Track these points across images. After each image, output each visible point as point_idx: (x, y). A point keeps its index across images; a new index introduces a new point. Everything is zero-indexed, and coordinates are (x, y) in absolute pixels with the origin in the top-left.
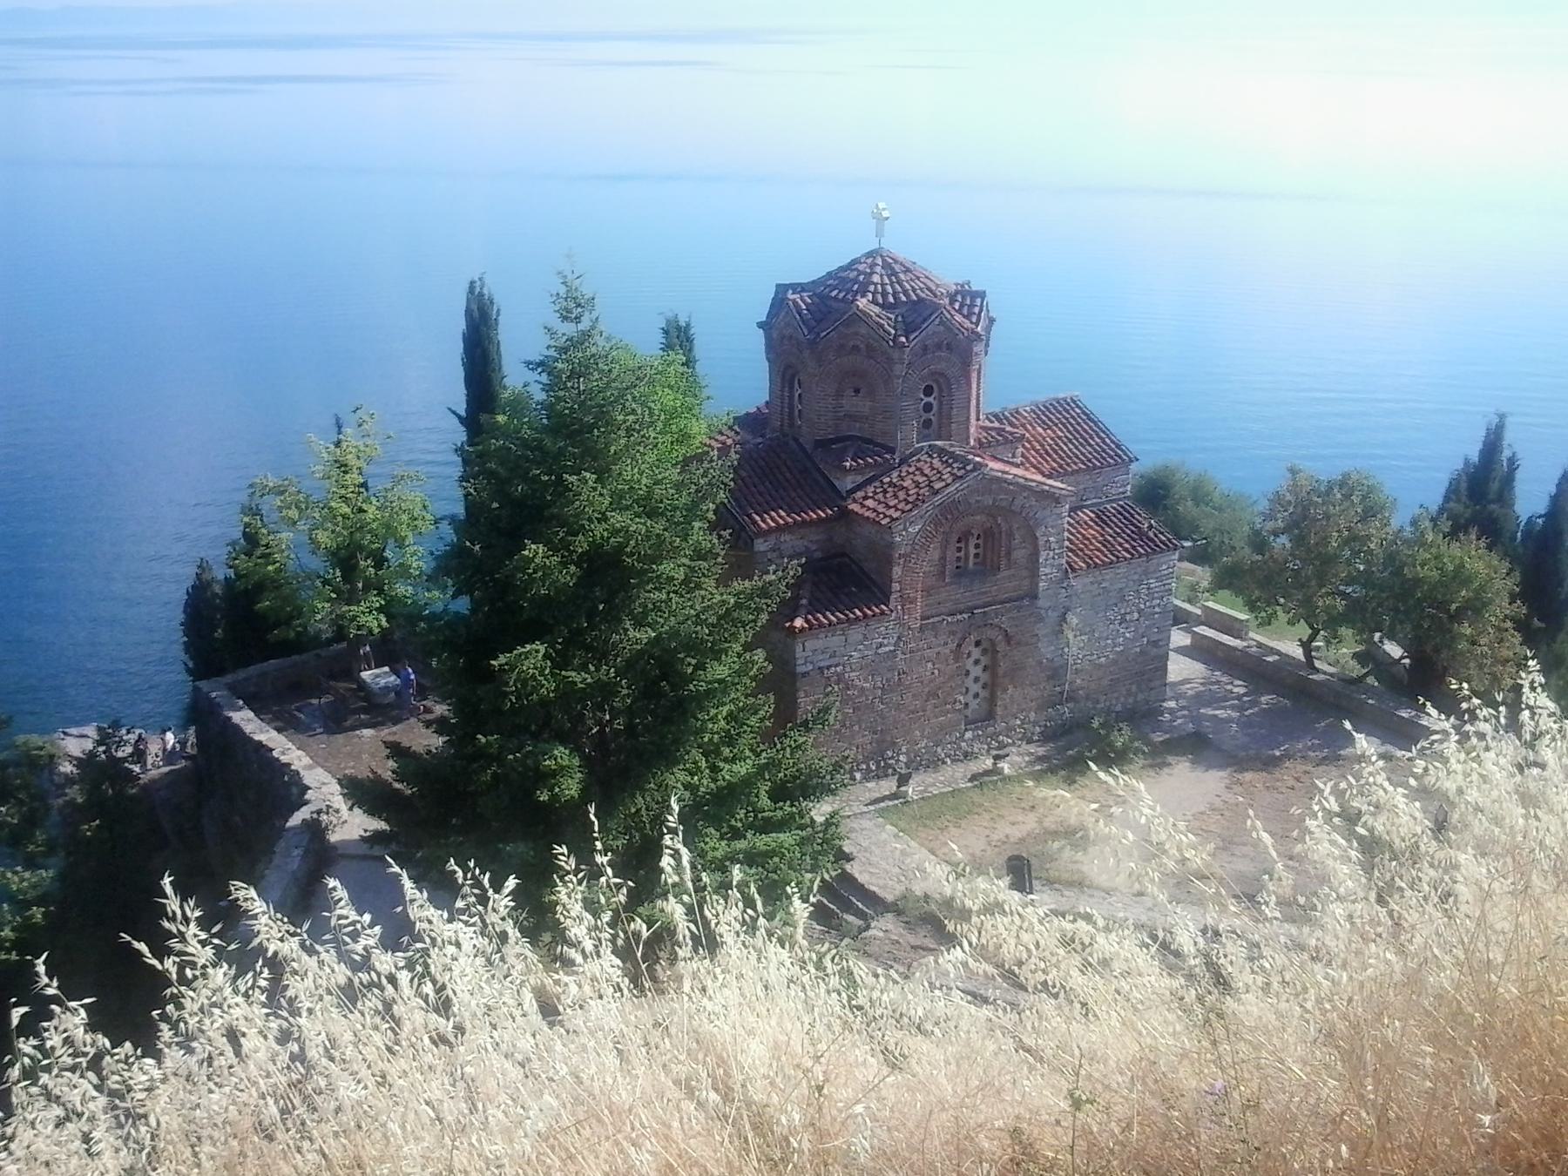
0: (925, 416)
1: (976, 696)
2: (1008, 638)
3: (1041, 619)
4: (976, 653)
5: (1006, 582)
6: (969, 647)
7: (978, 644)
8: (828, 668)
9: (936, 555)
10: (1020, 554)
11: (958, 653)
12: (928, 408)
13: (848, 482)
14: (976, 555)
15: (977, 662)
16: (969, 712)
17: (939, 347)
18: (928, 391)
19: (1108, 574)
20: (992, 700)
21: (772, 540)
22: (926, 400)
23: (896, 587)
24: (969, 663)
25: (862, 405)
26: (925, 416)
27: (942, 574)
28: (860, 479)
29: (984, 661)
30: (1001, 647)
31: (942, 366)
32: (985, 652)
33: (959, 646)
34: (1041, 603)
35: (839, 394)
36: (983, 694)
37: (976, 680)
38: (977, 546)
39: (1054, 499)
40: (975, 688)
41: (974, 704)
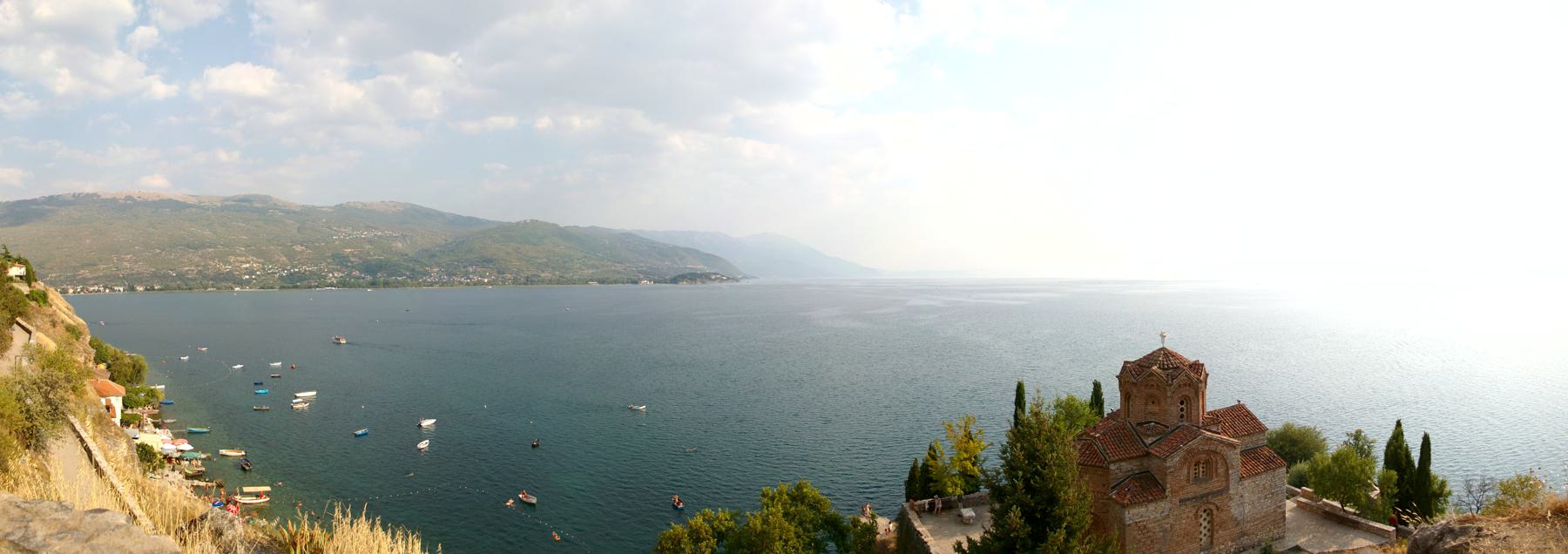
5: (1215, 484)
9: (1185, 471)
10: (1221, 471)
11: (1196, 516)
13: (1149, 441)
20: (1212, 537)
25: (1155, 408)
39: (1233, 446)
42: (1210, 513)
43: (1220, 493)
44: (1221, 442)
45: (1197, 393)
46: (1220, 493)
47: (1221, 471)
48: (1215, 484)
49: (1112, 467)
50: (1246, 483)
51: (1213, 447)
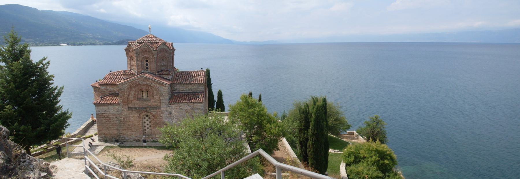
1: (148, 128)
2: (154, 116)
4: (147, 118)
6: (141, 116)
7: (147, 116)
12: (147, 65)
15: (147, 120)
16: (146, 131)
18: (147, 61)
24: (145, 120)
27: (134, 98)
29: (149, 120)
31: (148, 56)
32: (149, 118)
34: (162, 109)
35: (130, 61)
36: (150, 128)
37: (148, 124)
40: (147, 126)
44: (154, 81)
46: (155, 108)
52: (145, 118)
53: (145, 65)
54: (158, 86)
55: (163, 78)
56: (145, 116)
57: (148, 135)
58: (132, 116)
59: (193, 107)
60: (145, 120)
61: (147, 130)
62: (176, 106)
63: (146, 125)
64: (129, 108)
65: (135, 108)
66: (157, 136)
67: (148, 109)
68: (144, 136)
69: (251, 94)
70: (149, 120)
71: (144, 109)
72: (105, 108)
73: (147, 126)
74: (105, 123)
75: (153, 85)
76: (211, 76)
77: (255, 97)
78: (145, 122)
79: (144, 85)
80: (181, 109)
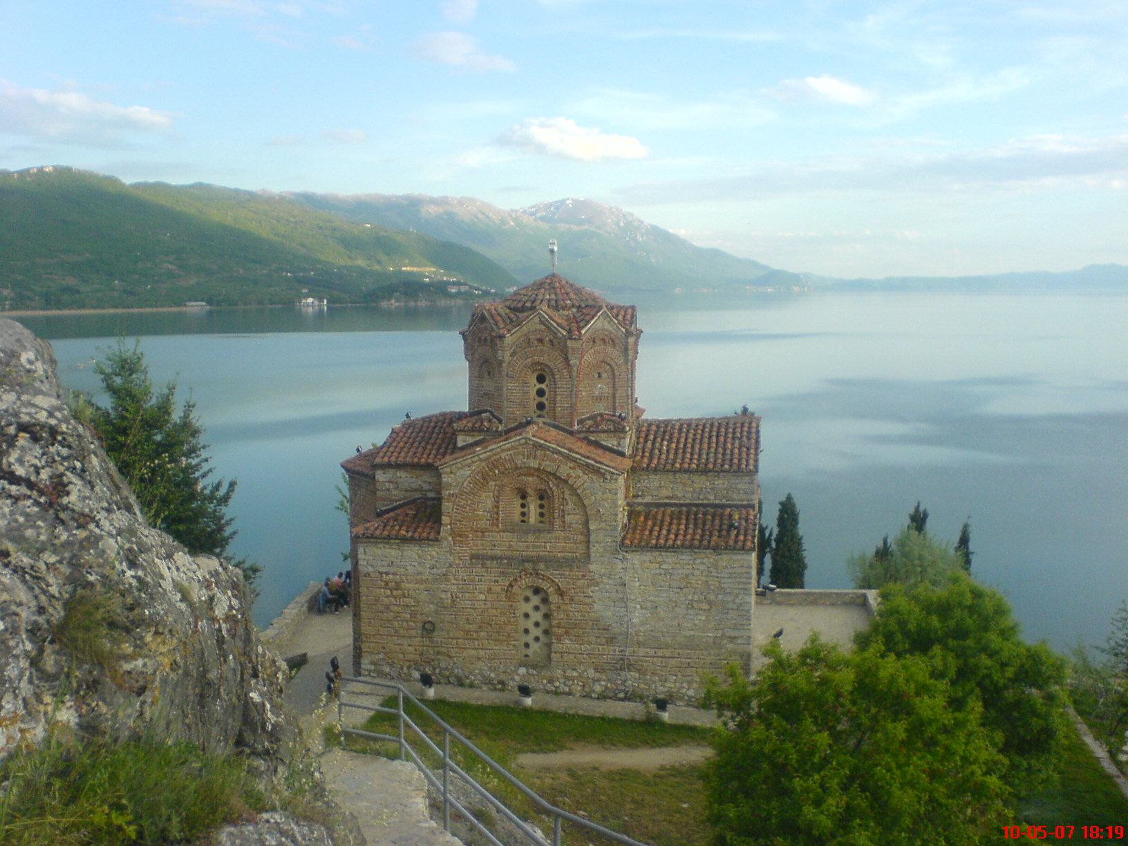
0: (538, 399)
1: (537, 639)
3: (597, 584)
4: (535, 600)
5: (556, 544)
7: (537, 591)
8: (387, 574)
9: (489, 503)
10: (574, 519)
12: (541, 393)
14: (542, 515)
15: (537, 608)
16: (530, 652)
17: (540, 341)
18: (541, 379)
19: (670, 559)
20: (549, 645)
21: (390, 474)
22: (539, 386)
23: (445, 520)
26: (538, 399)
27: (495, 520)
28: (470, 440)
29: (543, 609)
30: (554, 598)
31: (544, 359)
33: (511, 585)
34: (592, 567)
35: (480, 377)
37: (537, 624)
38: (541, 506)
39: (597, 471)
40: (535, 632)
41: (535, 647)
42: (545, 601)
43: (569, 563)
45: (567, 360)
46: (569, 563)
47: (574, 519)
48: (556, 544)
49: (380, 476)
50: (636, 559)
51: (549, 466)
52: (527, 599)
53: (533, 393)
54: (581, 479)
55: (597, 445)
56: (529, 593)
57: (534, 667)
58: (484, 587)
59: (716, 566)
60: (528, 608)
61: (535, 647)
62: (648, 556)
63: (529, 624)
64: (473, 557)
65: (493, 558)
66: (569, 673)
67: (542, 566)
68: (522, 671)
69: (919, 520)
70: (543, 609)
71: (528, 566)
72: (392, 552)
73: (535, 632)
74: (387, 607)
75: (564, 471)
76: (761, 439)
77: (941, 533)
78: (527, 616)
79: (530, 472)
80: (667, 572)
